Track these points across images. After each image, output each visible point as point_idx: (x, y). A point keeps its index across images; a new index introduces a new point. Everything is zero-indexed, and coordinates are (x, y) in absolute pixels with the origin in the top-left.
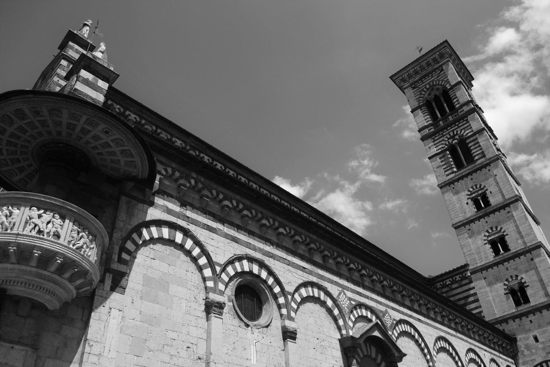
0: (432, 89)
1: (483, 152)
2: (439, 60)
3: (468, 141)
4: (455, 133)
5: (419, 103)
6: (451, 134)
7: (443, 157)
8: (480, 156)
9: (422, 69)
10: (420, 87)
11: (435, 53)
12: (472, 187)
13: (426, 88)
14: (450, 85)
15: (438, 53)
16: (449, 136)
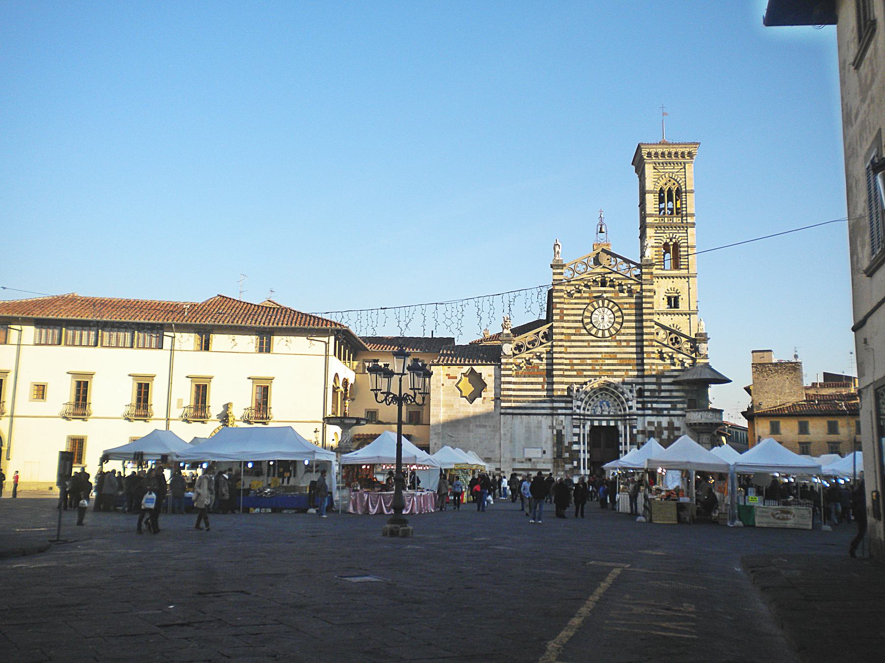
0: (670, 181)
1: (688, 265)
2: (686, 156)
3: (681, 249)
4: (674, 236)
5: (654, 188)
6: (671, 236)
7: (658, 251)
8: (684, 267)
9: (670, 153)
10: (660, 171)
11: (686, 148)
12: (671, 288)
13: (665, 177)
14: (686, 188)
15: (688, 149)
16: (668, 236)
